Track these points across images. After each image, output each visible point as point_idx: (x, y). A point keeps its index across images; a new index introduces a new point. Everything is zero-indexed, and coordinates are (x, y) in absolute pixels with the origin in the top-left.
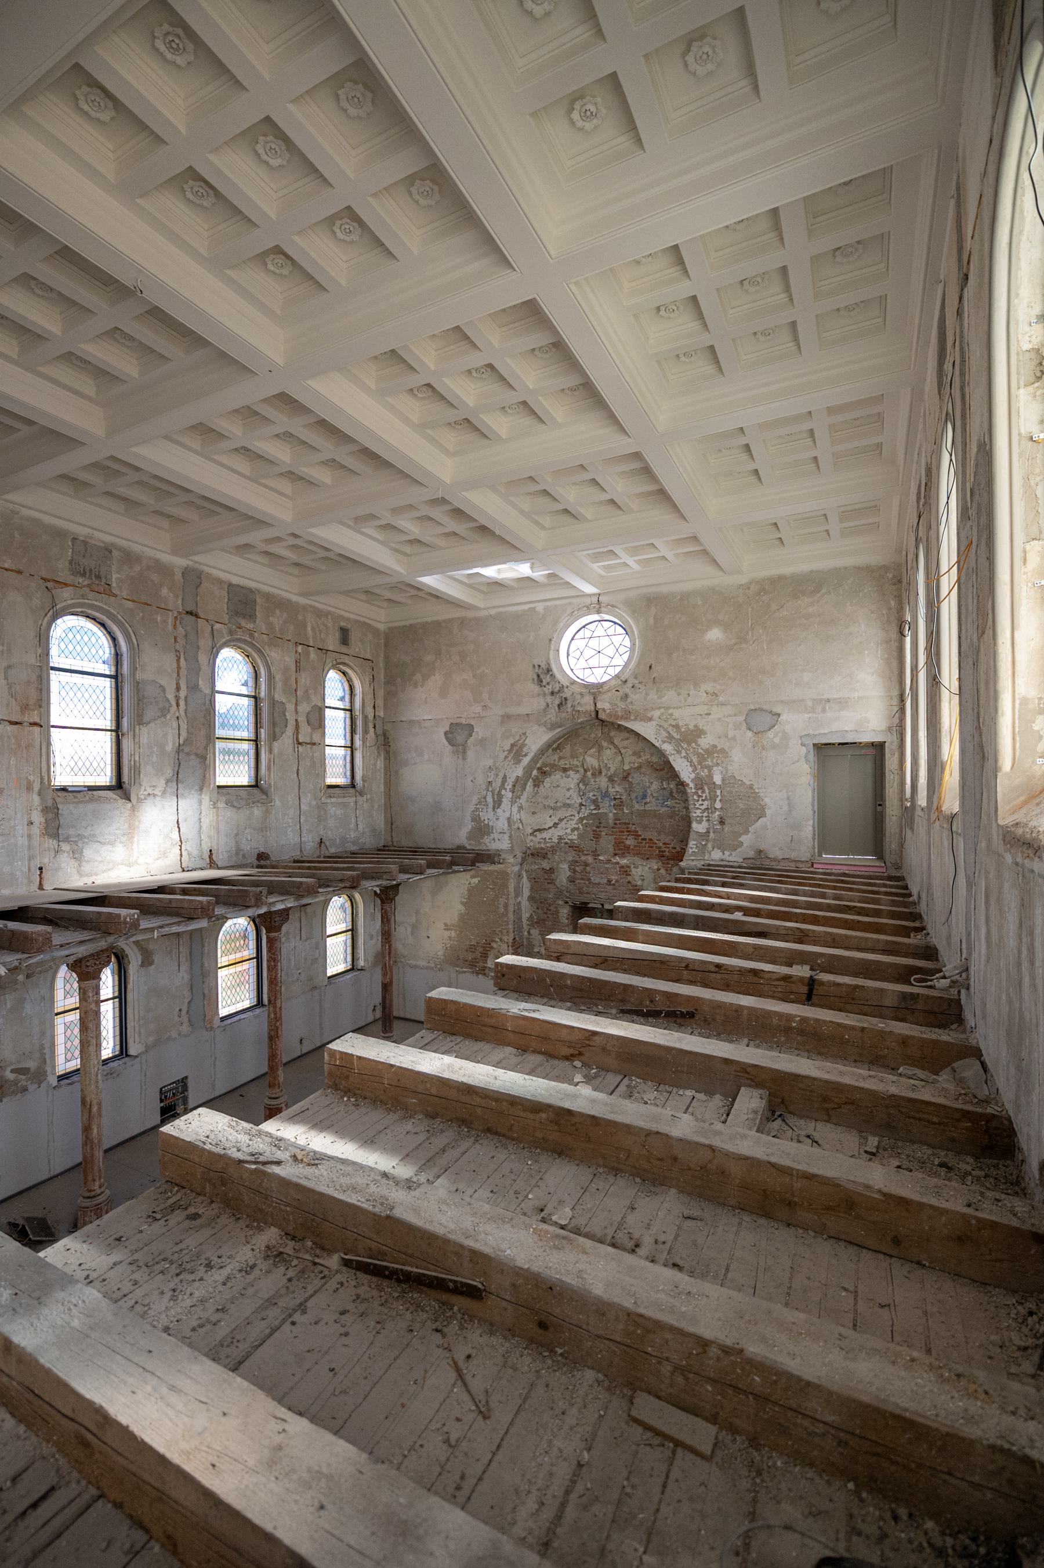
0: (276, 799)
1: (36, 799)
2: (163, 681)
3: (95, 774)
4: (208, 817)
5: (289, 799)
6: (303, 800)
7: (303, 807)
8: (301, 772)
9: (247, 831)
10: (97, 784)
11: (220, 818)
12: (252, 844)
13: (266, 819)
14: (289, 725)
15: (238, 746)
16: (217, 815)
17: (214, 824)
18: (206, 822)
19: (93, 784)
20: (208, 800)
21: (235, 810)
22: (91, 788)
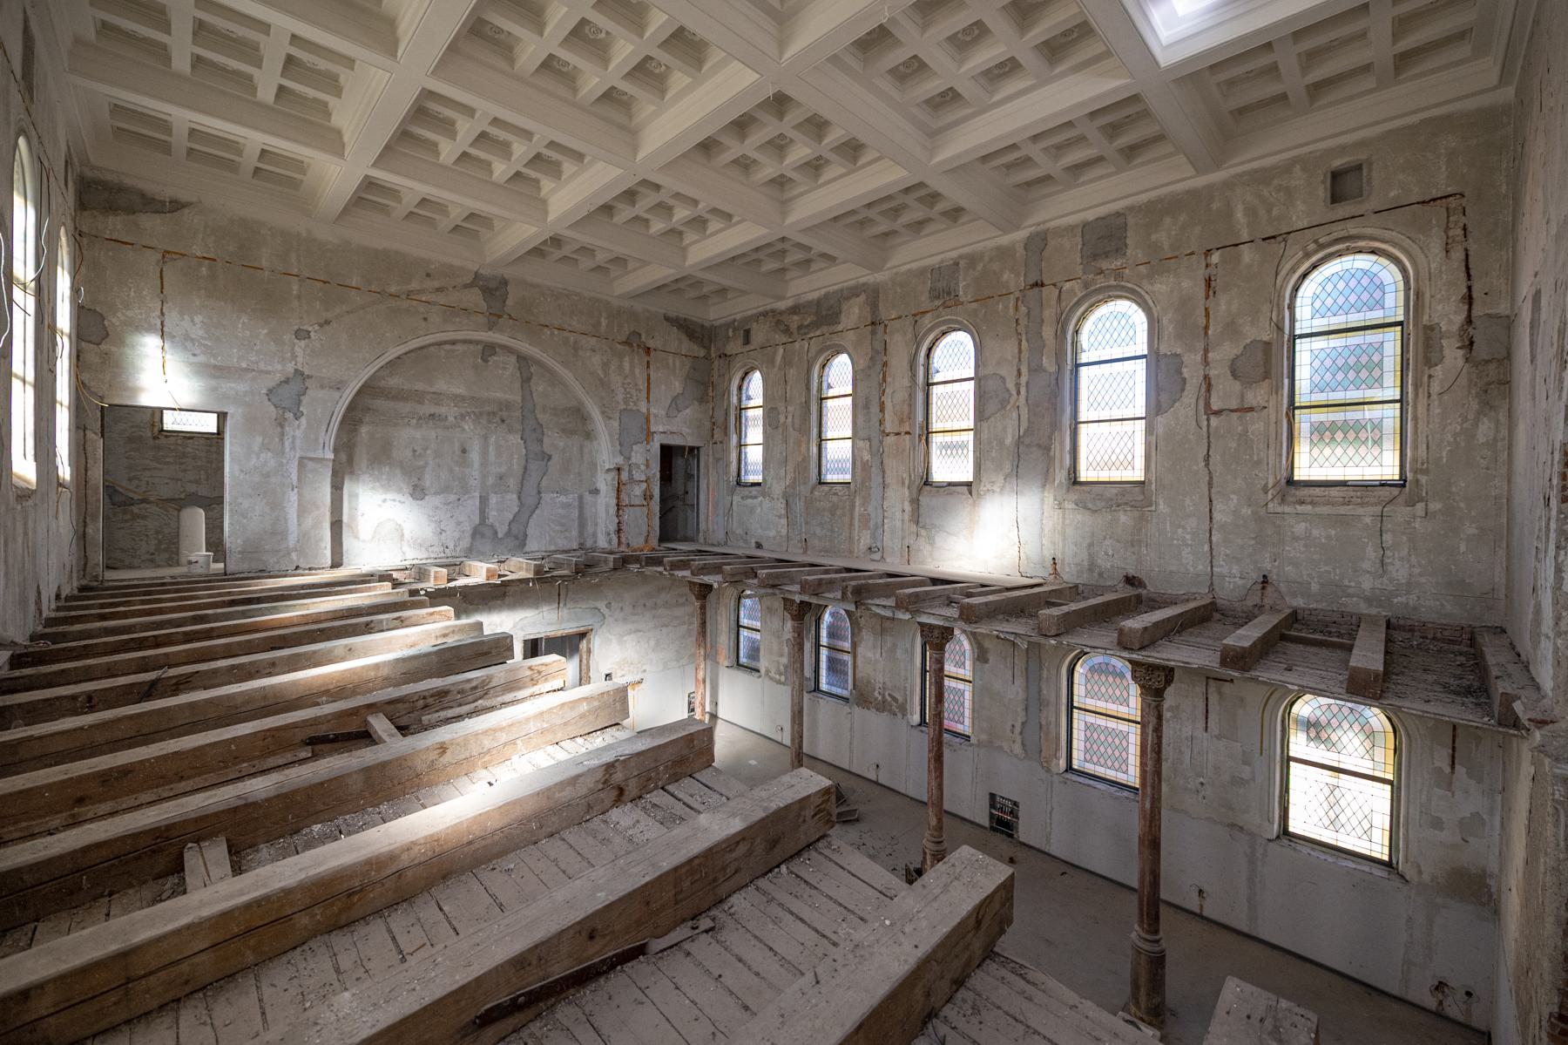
0: (1161, 502)
1: (906, 492)
2: (1003, 373)
3: (1121, 467)
4: (1052, 518)
5: (1188, 501)
6: (1218, 506)
7: (1217, 516)
8: (1215, 458)
9: (1107, 542)
10: (1329, 478)
11: (1067, 522)
12: (1116, 561)
13: (1140, 529)
14: (1188, 387)
15: (956, 438)
16: (1064, 518)
17: (1059, 528)
18: (1049, 525)
19: (1324, 478)
20: (1051, 499)
21: (1087, 513)
22: (950, 484)
